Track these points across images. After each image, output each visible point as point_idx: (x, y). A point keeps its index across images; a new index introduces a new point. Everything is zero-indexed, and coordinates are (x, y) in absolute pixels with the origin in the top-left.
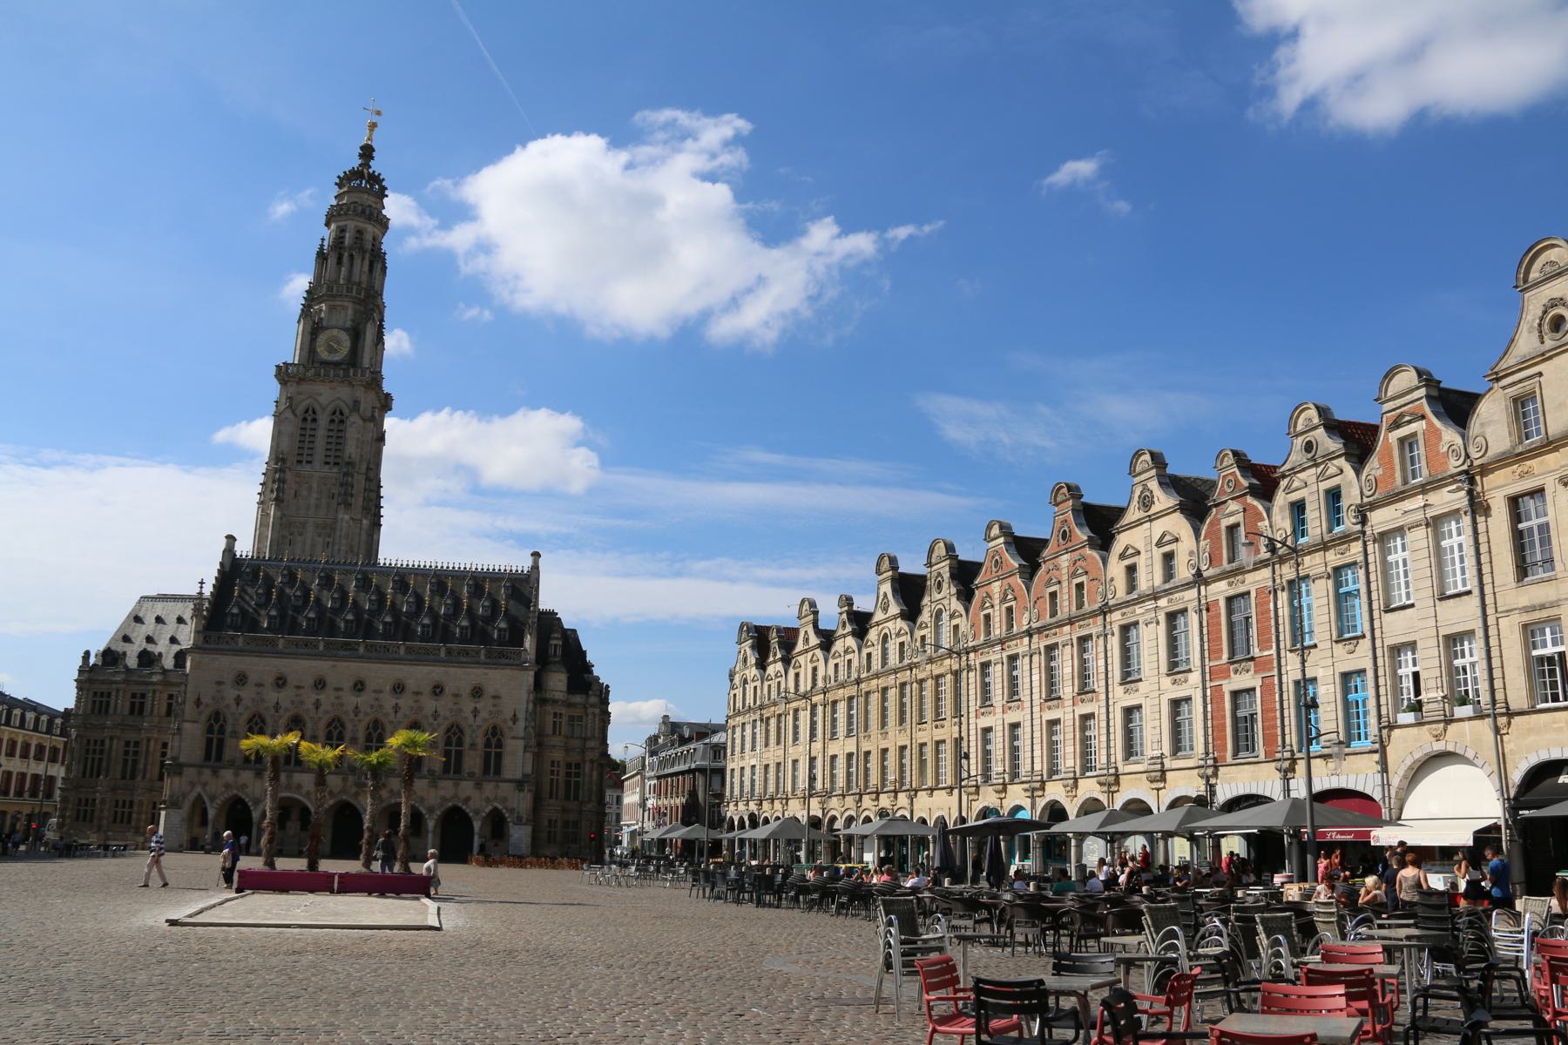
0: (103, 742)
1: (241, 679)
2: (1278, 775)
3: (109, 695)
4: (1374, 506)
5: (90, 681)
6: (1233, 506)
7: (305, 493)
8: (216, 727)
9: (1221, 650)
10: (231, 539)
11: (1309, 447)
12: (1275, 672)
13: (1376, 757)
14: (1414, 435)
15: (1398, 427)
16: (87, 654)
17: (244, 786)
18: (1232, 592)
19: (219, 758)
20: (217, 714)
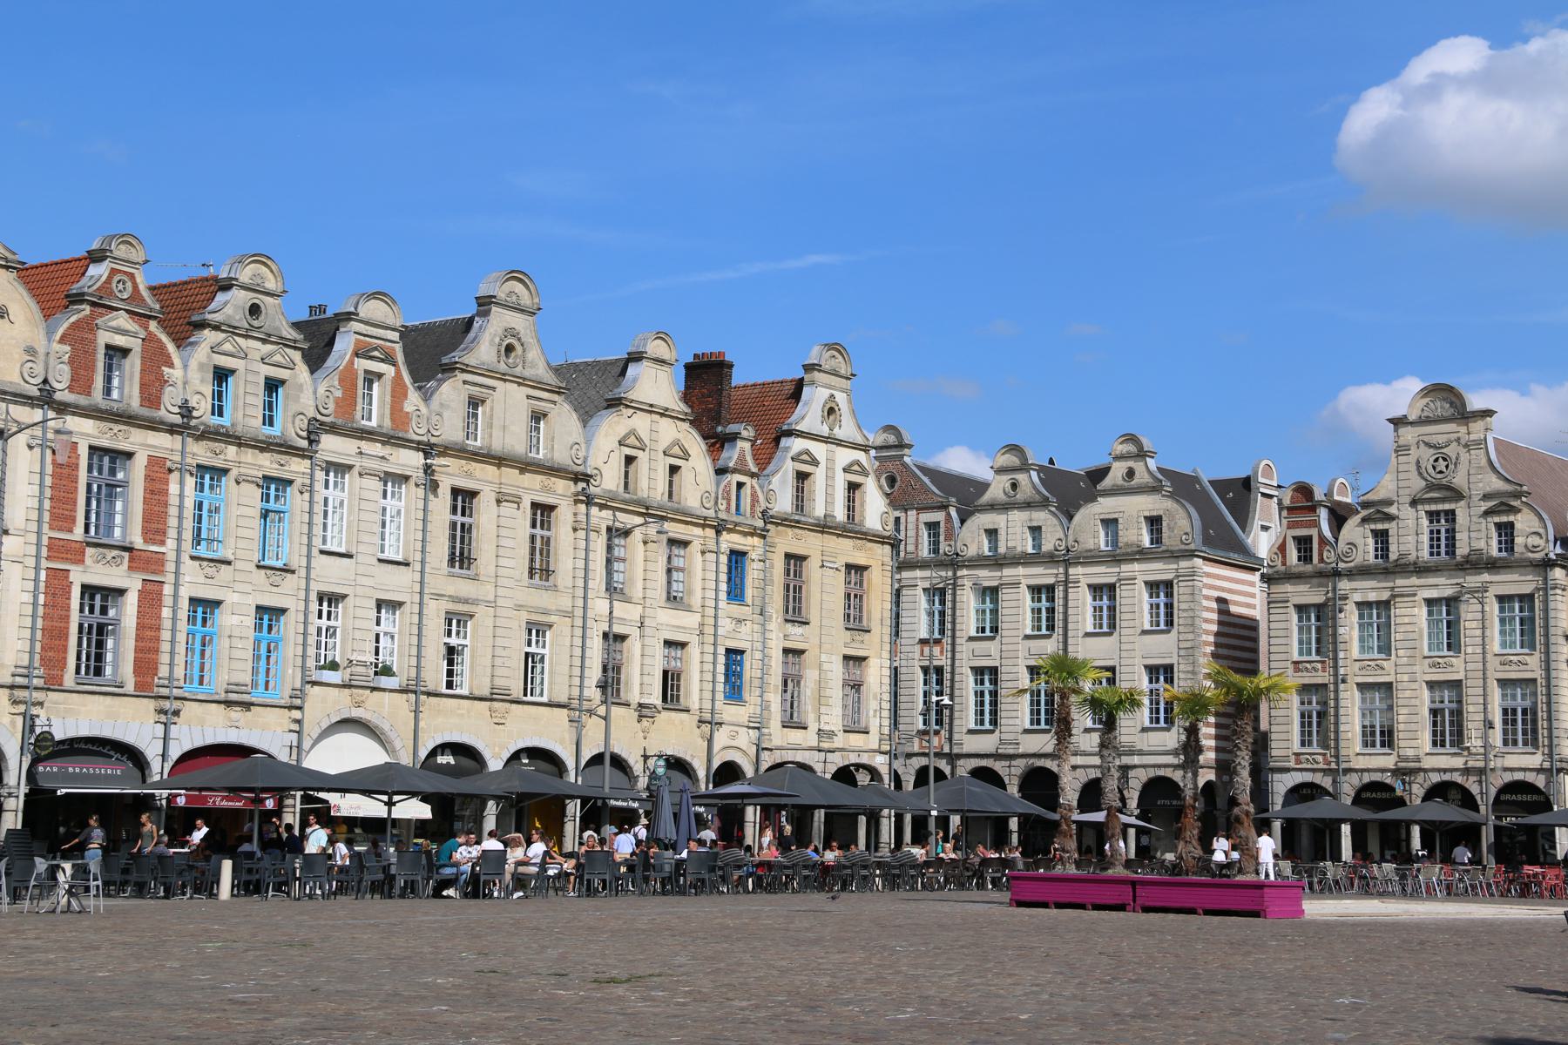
2: (153, 717)
4: (333, 429)
6: (122, 320)
9: (74, 520)
11: (255, 310)
12: (170, 578)
13: (296, 714)
14: (380, 376)
15: (371, 358)
18: (105, 443)
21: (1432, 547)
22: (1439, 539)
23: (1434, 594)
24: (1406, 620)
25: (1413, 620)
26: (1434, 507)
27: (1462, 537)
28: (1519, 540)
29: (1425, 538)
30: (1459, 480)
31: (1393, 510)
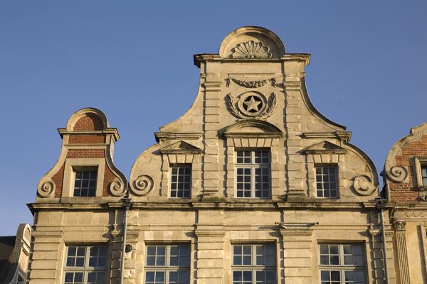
21: (239, 186)
22: (248, 179)
23: (245, 236)
24: (211, 264)
25: (219, 264)
26: (245, 143)
27: (277, 176)
28: (344, 183)
29: (233, 175)
30: (274, 118)
31: (198, 143)
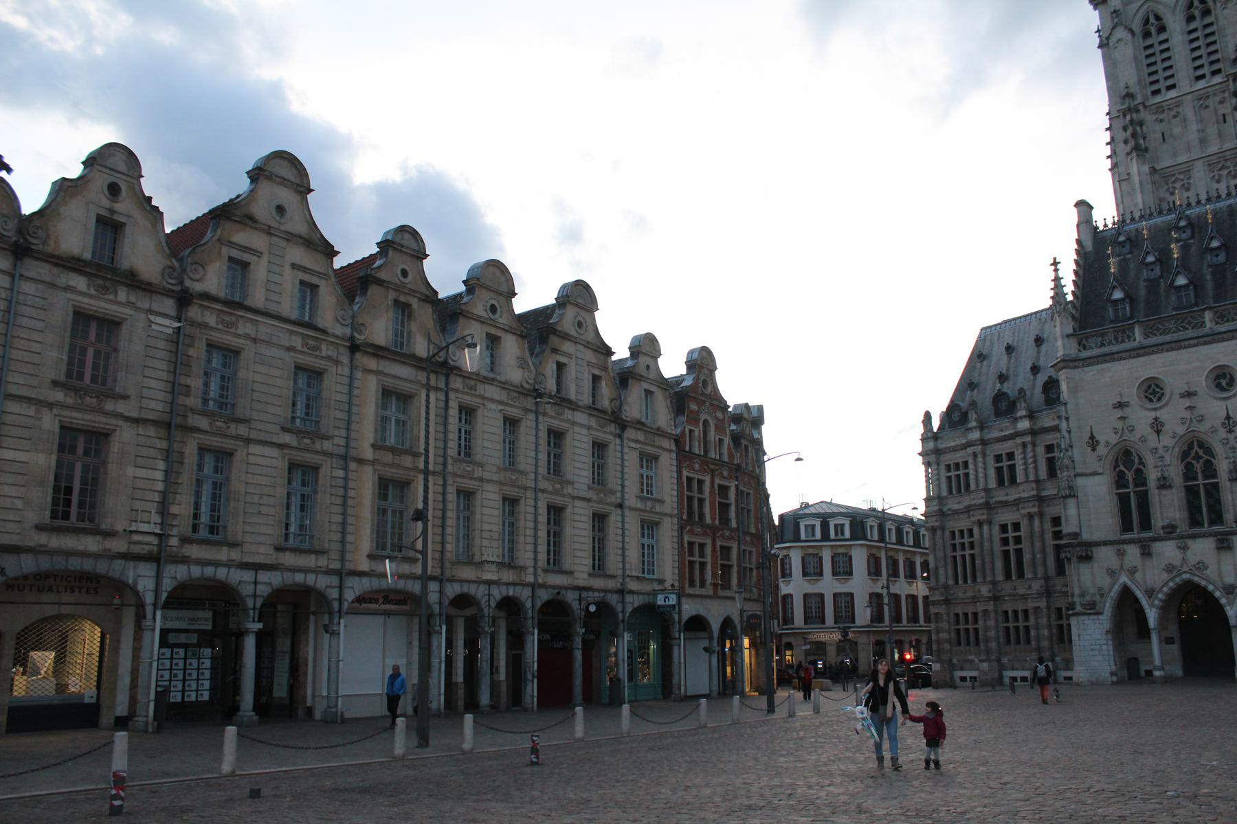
0: (971, 531)
1: (1153, 390)
3: (966, 464)
5: (937, 452)
7: (1177, 130)
8: (1130, 476)
10: (1084, 207)
16: (928, 417)
17: (1201, 566)
19: (1146, 524)
20: (1127, 453)
